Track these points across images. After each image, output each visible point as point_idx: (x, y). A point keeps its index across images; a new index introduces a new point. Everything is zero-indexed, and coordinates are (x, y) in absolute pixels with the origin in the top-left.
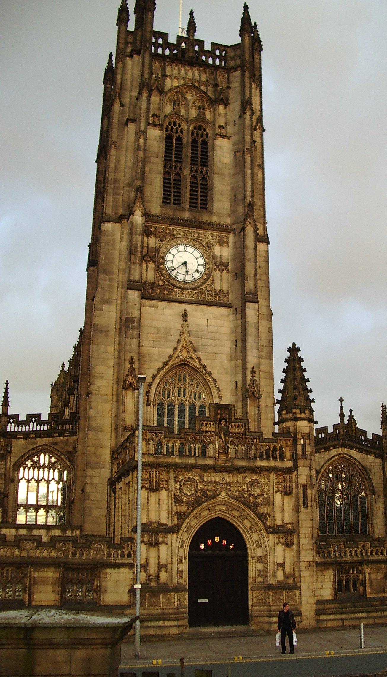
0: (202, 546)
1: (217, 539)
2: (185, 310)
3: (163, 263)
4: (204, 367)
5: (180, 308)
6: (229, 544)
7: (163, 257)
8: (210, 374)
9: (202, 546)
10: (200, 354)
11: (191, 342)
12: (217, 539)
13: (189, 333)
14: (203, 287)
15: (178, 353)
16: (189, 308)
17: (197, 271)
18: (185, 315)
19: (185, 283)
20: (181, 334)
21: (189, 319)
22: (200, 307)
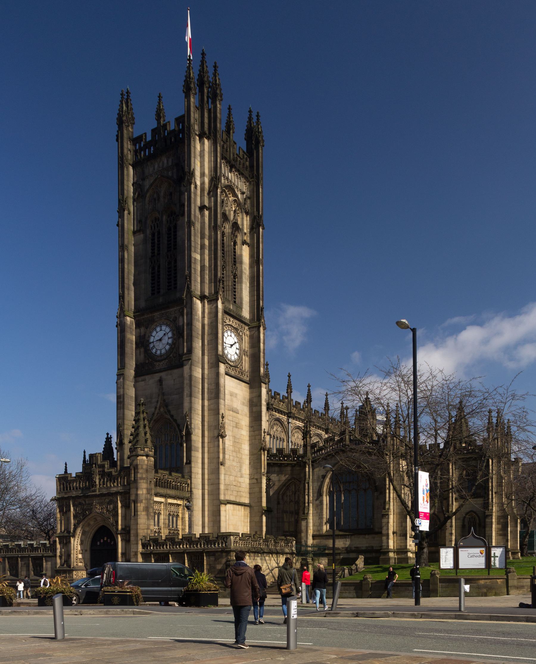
0: (98, 543)
1: (105, 539)
2: (161, 377)
3: (148, 346)
4: (172, 416)
5: (157, 376)
6: (111, 541)
7: (148, 341)
8: (175, 421)
9: (98, 543)
10: (170, 408)
11: (164, 401)
12: (105, 539)
13: (163, 394)
14: (171, 356)
15: (157, 409)
16: (163, 374)
17: (168, 343)
18: (160, 381)
19: (161, 355)
20: (159, 395)
21: (163, 383)
22: (170, 372)
